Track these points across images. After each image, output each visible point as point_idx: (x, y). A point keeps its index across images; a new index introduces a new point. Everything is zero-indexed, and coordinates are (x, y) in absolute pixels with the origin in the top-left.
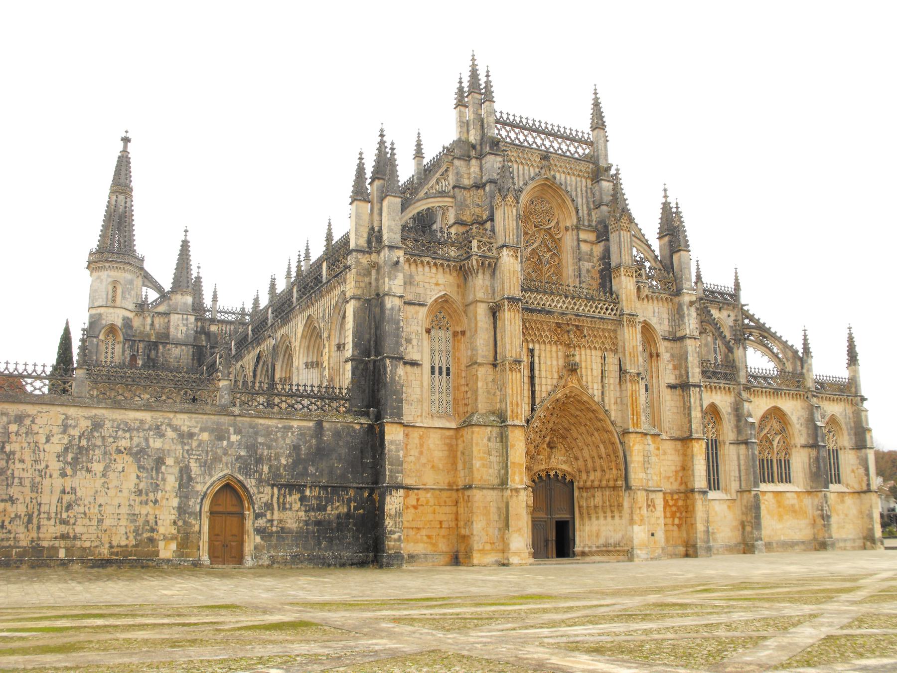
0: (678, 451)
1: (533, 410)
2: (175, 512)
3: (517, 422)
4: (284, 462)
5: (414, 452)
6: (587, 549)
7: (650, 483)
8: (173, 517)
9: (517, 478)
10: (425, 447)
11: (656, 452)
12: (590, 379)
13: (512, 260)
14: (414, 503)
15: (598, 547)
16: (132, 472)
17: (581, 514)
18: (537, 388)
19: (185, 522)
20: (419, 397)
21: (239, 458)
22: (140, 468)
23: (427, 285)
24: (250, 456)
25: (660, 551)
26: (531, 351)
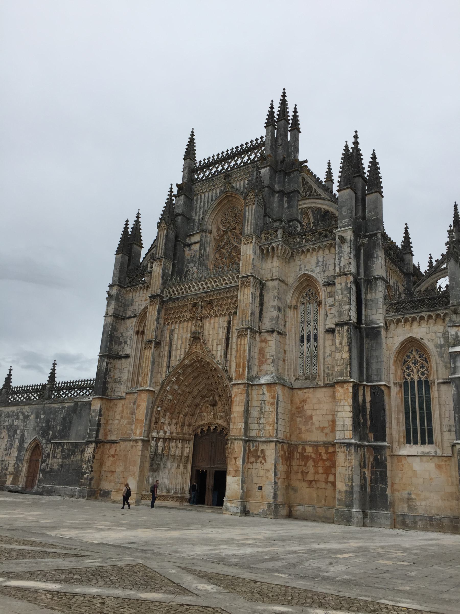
2: (15, 459)
4: (58, 429)
5: (118, 417)
7: (261, 434)
8: (14, 462)
9: (138, 432)
13: (158, 268)
14: (113, 453)
16: (6, 438)
18: (173, 358)
19: (18, 465)
21: (43, 427)
22: (9, 436)
23: (140, 303)
24: (46, 426)
25: (266, 508)
26: (173, 330)
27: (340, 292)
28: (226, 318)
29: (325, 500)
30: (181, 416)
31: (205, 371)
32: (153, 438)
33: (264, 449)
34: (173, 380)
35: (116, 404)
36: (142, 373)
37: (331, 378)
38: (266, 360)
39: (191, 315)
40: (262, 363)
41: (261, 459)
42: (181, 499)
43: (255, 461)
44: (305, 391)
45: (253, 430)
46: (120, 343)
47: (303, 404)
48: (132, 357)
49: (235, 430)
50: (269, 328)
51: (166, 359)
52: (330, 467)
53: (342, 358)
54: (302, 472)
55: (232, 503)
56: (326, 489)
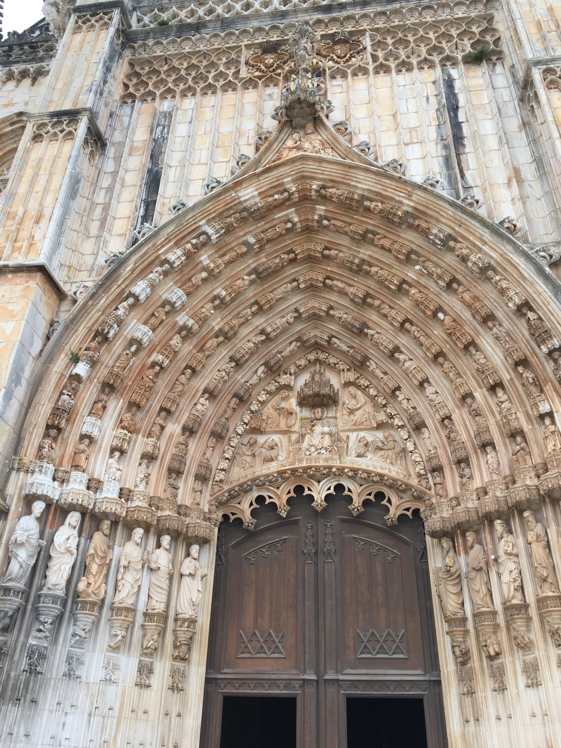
26: (168, 115)
32: (29, 500)
34: (171, 257)
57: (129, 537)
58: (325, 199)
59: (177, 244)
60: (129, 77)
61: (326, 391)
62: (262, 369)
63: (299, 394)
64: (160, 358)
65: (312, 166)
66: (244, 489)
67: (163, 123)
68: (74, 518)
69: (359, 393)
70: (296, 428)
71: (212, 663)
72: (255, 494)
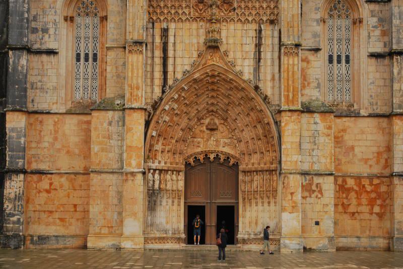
0: (383, 129)
1: (163, 92)
3: (135, 105)
5: (48, 139)
6: (246, 237)
9: (134, 163)
10: (60, 132)
11: (326, 131)
12: (239, 55)
14: (47, 187)
15: (256, 235)
17: (244, 199)
18: (170, 68)
20: (55, 84)
25: (326, 241)
27: (398, 16)
28: (254, 26)
29: (370, 230)
30: (174, 141)
31: (216, 88)
33: (320, 183)
35: (40, 119)
36: (349, 114)
37: (375, 107)
38: (309, 84)
39: (197, 14)
40: (304, 87)
41: (316, 194)
42: (179, 240)
43: (308, 195)
44: (344, 119)
45: (304, 162)
46: (35, 31)
47: (342, 133)
48: (63, 53)
49: (289, 163)
50: (311, 45)
51: (158, 69)
52: (375, 198)
53: (401, 90)
54: (343, 204)
55: (293, 240)
56: (370, 220)
57: (167, 174)
58: (218, 76)
59: (176, 93)
60: (149, 7)
61: (215, 127)
62: (196, 119)
63: (207, 126)
64: (171, 124)
65: (216, 67)
66: (191, 155)
67: (165, 32)
68: (157, 172)
69: (224, 126)
70: (205, 137)
71: (185, 199)
72: (194, 156)
